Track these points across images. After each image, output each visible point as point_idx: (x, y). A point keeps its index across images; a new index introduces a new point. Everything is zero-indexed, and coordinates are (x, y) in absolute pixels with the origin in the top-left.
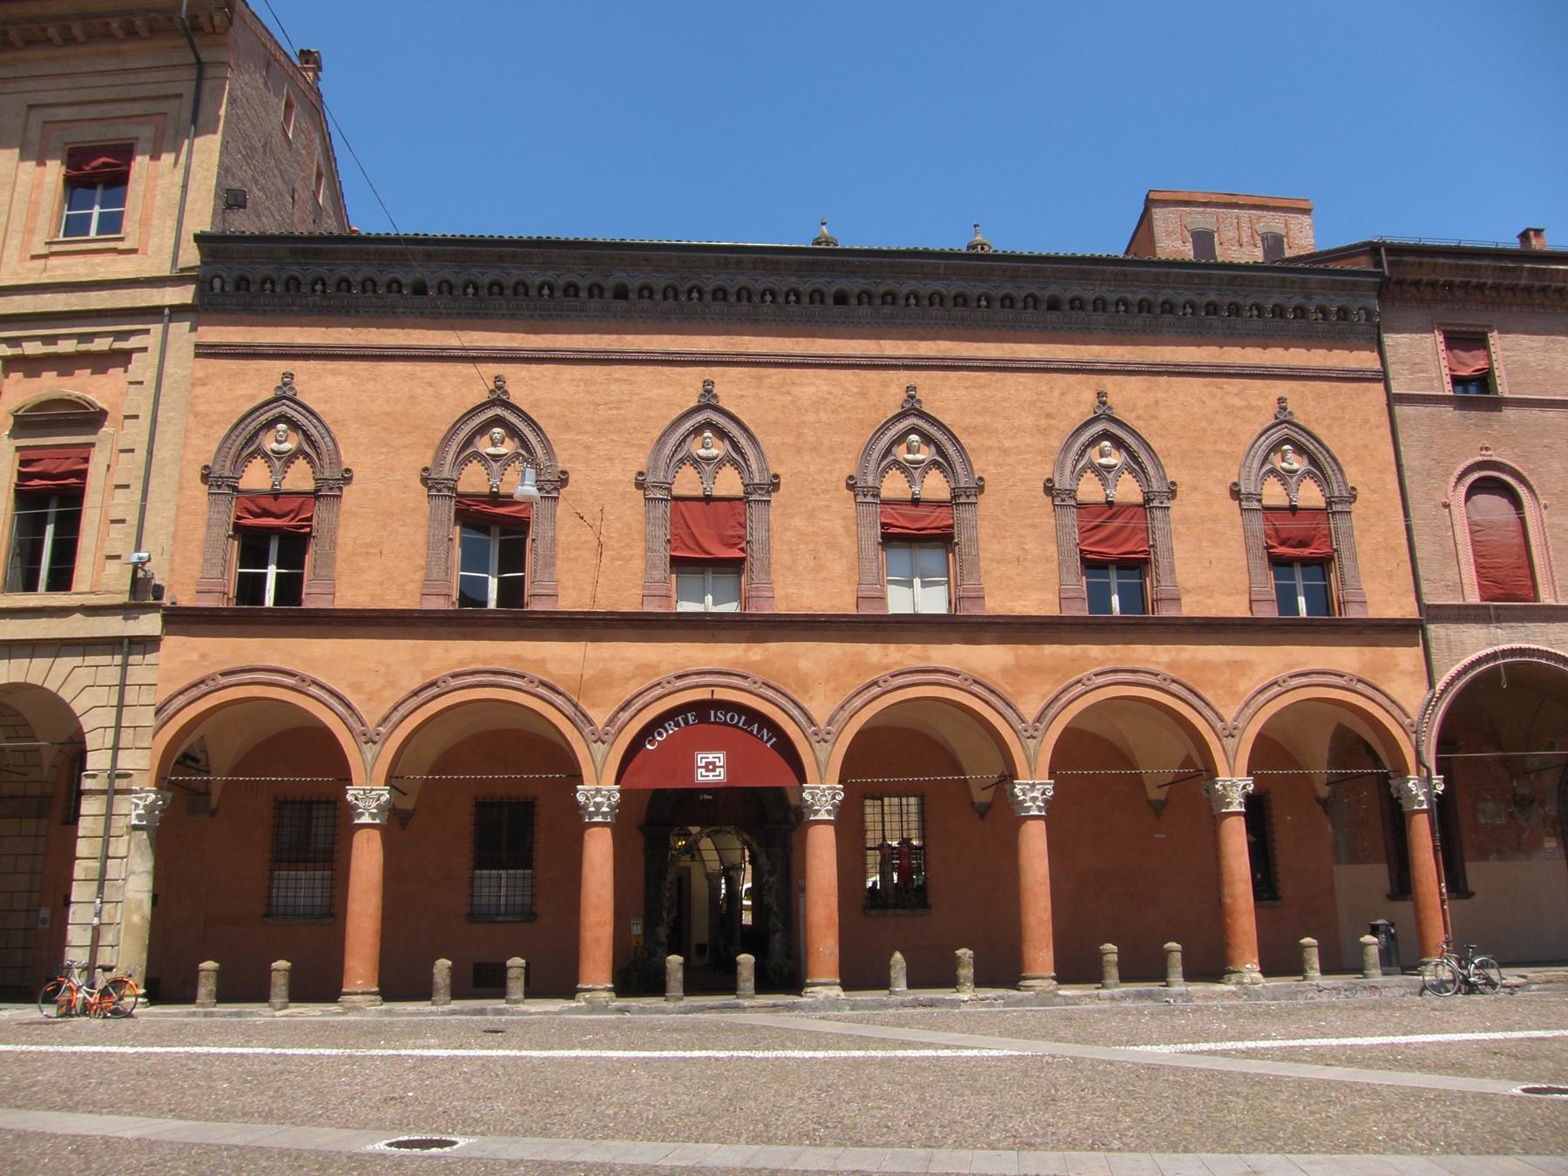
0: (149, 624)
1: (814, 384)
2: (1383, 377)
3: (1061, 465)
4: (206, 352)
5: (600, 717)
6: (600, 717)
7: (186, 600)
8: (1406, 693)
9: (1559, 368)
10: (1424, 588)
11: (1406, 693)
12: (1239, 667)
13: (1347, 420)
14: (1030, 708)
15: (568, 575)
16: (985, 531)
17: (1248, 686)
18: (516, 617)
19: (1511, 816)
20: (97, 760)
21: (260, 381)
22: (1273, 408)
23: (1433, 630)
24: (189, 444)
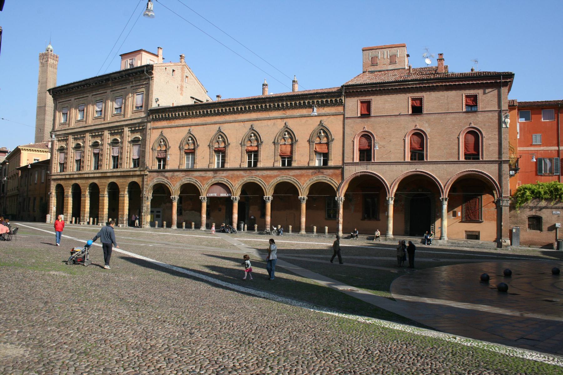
9: (386, 107)
10: (345, 159)
13: (334, 126)
23: (346, 168)
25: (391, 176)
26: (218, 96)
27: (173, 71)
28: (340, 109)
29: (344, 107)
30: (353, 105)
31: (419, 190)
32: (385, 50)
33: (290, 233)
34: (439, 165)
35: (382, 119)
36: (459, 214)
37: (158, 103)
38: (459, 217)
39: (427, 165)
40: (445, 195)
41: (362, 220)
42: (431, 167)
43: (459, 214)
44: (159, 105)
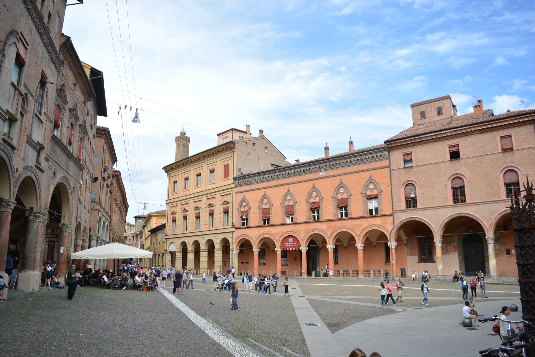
0: (233, 230)
1: (301, 185)
2: (389, 167)
3: (334, 194)
4: (237, 193)
5: (277, 239)
6: (277, 239)
7: (237, 226)
8: (389, 227)
10: (394, 207)
11: (389, 227)
12: (361, 225)
14: (329, 234)
15: (274, 220)
16: (324, 206)
17: (362, 228)
18: (269, 226)
19: (446, 246)
20: (231, 247)
21: (241, 196)
22: (369, 176)
23: (395, 215)
24: (236, 206)
25: (436, 221)
26: (296, 161)
27: (254, 144)
28: (386, 163)
29: (389, 160)
30: (397, 156)
31: (470, 231)
32: (432, 104)
33: (351, 277)
34: (481, 206)
35: (424, 167)
36: (513, 251)
37: (241, 171)
38: (513, 255)
39: (470, 207)
40: (490, 235)
41: (418, 263)
42: (474, 208)
43: (513, 251)
44: (242, 173)
